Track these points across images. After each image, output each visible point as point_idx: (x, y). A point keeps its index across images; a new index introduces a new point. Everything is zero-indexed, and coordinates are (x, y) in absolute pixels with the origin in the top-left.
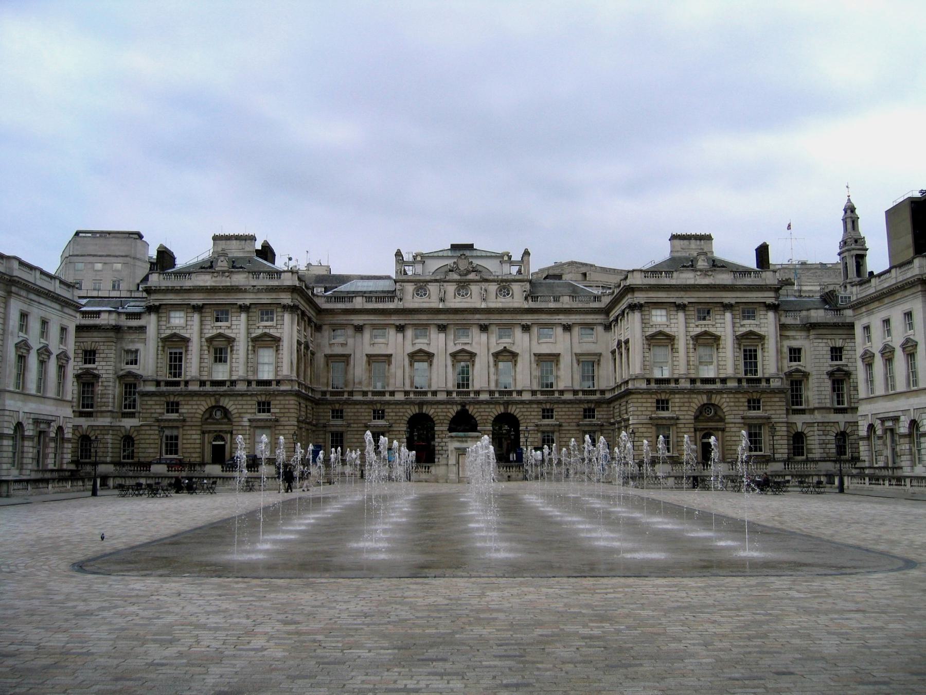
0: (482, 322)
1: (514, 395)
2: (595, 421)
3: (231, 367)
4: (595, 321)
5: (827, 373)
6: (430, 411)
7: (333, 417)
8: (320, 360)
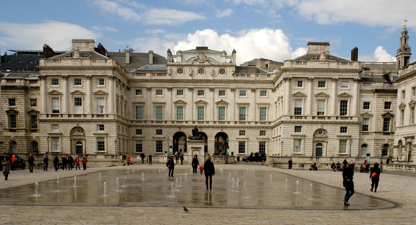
1: (226, 123)
2: (265, 137)
3: (84, 108)
5: (382, 115)
8: (130, 105)
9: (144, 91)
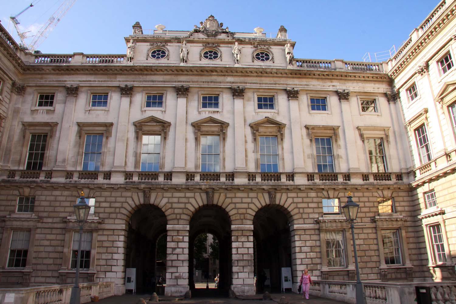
0: (235, 86)
6: (161, 200)
7: (20, 210)
9: (59, 97)
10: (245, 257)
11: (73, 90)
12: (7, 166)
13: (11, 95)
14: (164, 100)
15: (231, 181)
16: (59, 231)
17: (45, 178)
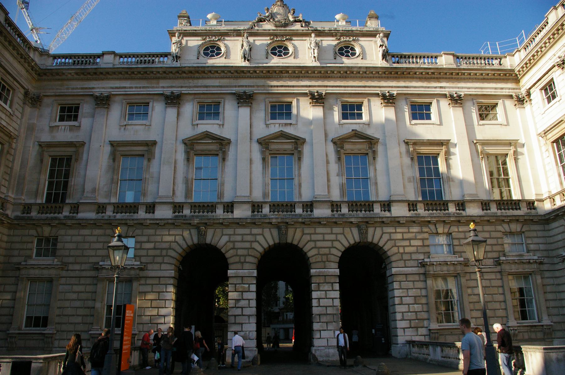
4: (499, 92)
6: (220, 239)
7: (38, 254)
9: (86, 108)
10: (330, 311)
11: (103, 100)
12: (20, 199)
13: (23, 108)
14: (221, 110)
15: (309, 213)
16: (88, 281)
17: (70, 213)
